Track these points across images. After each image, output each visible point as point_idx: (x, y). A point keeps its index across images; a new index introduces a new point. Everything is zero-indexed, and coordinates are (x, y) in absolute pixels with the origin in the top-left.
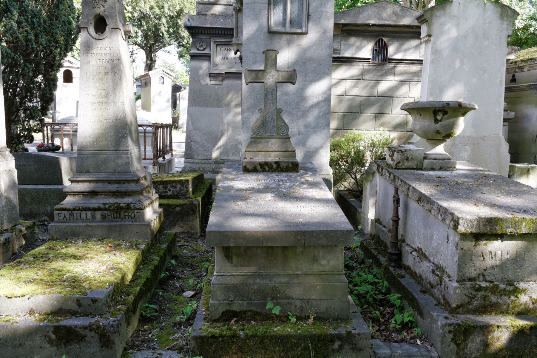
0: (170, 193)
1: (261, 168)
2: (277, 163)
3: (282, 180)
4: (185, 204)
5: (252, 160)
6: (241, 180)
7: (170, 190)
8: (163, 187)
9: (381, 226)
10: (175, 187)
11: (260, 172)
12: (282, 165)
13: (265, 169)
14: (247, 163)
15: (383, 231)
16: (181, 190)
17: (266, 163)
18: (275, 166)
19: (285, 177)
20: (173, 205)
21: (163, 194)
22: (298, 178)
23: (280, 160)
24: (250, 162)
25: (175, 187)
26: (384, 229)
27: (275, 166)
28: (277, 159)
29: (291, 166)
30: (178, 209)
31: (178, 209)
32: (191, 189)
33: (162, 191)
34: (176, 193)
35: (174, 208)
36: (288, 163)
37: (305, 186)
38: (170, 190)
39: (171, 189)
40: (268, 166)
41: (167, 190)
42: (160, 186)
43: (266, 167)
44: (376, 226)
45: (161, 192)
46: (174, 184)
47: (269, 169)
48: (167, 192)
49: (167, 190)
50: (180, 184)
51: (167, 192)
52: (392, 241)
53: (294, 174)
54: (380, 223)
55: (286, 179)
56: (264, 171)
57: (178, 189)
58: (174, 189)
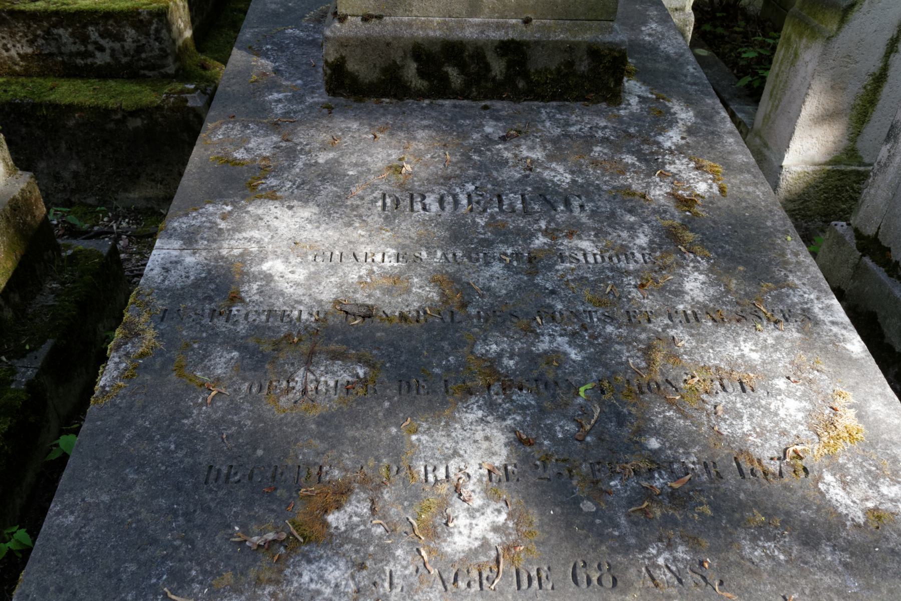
0: (101, 59)
1: (421, 74)
2: (511, 49)
3: (547, 196)
4: (159, 108)
5: (374, 29)
7: (101, 49)
8: (72, 35)
11: (420, 95)
12: (539, 62)
13: (445, 78)
14: (343, 43)
16: (140, 49)
17: (454, 50)
18: (498, 67)
20: (115, 111)
21: (80, 61)
23: (528, 34)
24: (365, 44)
27: (498, 67)
28: (512, 28)
29: (583, 66)
30: (137, 123)
31: (137, 123)
33: (74, 48)
34: (124, 60)
35: (123, 120)
36: (571, 48)
38: (101, 49)
39: (102, 42)
40: (462, 67)
41: (91, 47)
42: (61, 31)
43: (453, 72)
44: (859, 270)
45: (71, 54)
46: (111, 24)
47: (468, 84)
48: (92, 55)
50: (133, 26)
51: (92, 55)
56: (439, 89)
57: (129, 44)
58: (117, 46)
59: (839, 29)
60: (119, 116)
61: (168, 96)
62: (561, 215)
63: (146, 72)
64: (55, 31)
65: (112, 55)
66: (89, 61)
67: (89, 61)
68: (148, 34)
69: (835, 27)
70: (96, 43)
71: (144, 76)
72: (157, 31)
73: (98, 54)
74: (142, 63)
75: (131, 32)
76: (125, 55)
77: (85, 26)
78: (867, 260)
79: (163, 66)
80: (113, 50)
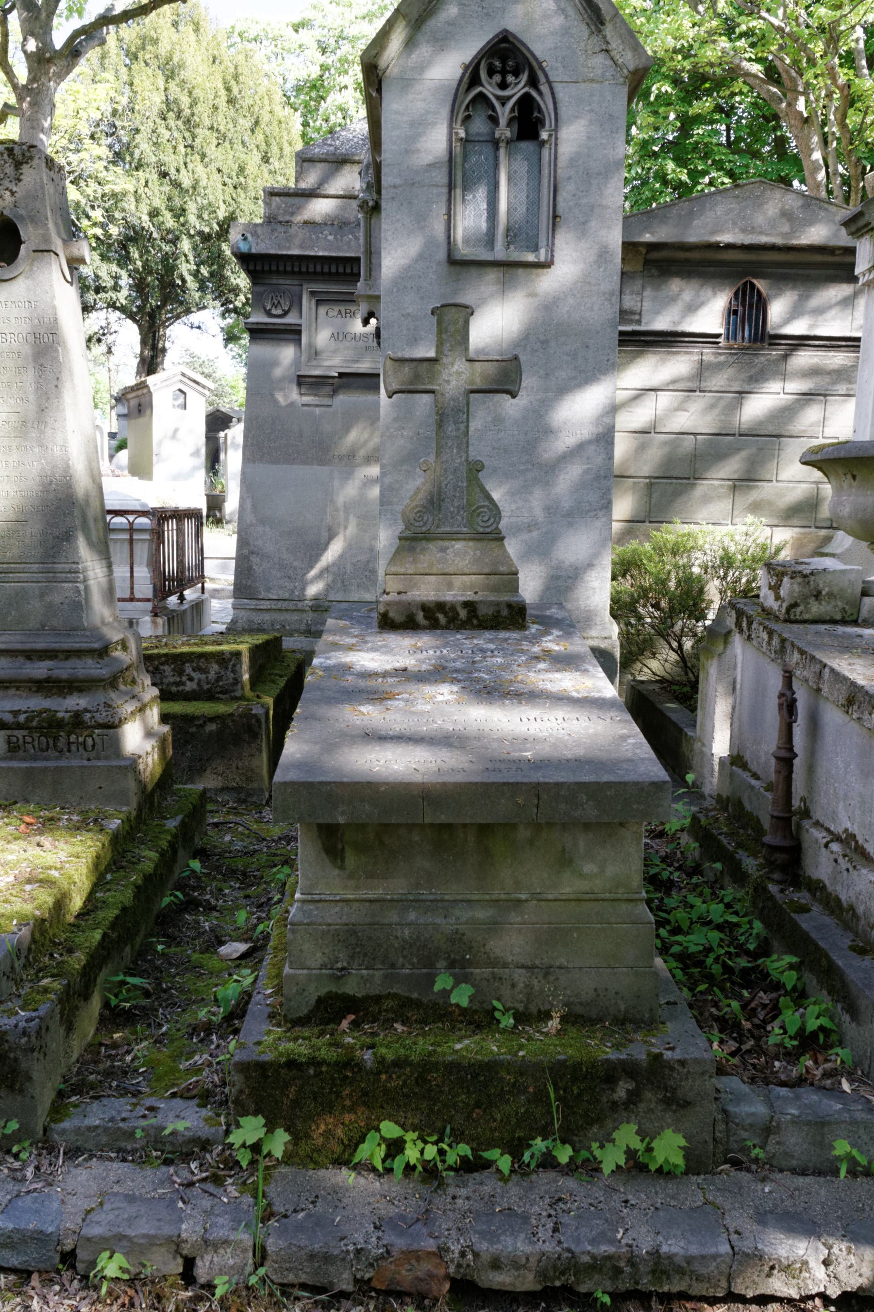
0: (190, 686)
1: (425, 617)
2: (467, 604)
3: (482, 651)
4: (231, 715)
5: (403, 597)
6: (374, 649)
7: (191, 679)
8: (173, 670)
9: (745, 775)
10: (205, 671)
11: (424, 628)
12: (482, 611)
13: (437, 620)
14: (388, 604)
15: (752, 787)
16: (219, 678)
17: (441, 606)
18: (463, 614)
19: (491, 641)
20: (198, 718)
21: (174, 689)
22: (525, 645)
23: (476, 598)
24: (398, 603)
25: (205, 671)
26: (754, 782)
27: (463, 614)
28: (469, 596)
29: (505, 612)
30: (212, 727)
31: (212, 727)
32: (246, 677)
33: (172, 680)
34: (206, 687)
35: (201, 726)
36: (498, 604)
37: (542, 666)
38: (191, 679)
39: (193, 674)
40: (445, 613)
41: (184, 678)
42: (166, 667)
43: (441, 618)
44: (732, 775)
45: (169, 684)
46: (202, 663)
47: (449, 622)
48: (184, 684)
49: (184, 678)
50: (217, 662)
51: (184, 684)
52: (775, 814)
53: (515, 635)
54: (744, 766)
55: (492, 646)
56: (433, 625)
57: (212, 675)
58: (203, 677)
59: (725, 648)
60: (201, 722)
61: (238, 707)
62: (489, 653)
63: (221, 696)
64: (162, 667)
65: (198, 684)
66: (181, 688)
67: (181, 688)
68: (227, 668)
69: (722, 647)
70: (188, 675)
71: (218, 699)
72: (234, 666)
73: (188, 683)
74: (219, 689)
75: (216, 667)
76: (208, 683)
77: (184, 663)
78: (734, 768)
79: (234, 691)
80: (200, 680)
